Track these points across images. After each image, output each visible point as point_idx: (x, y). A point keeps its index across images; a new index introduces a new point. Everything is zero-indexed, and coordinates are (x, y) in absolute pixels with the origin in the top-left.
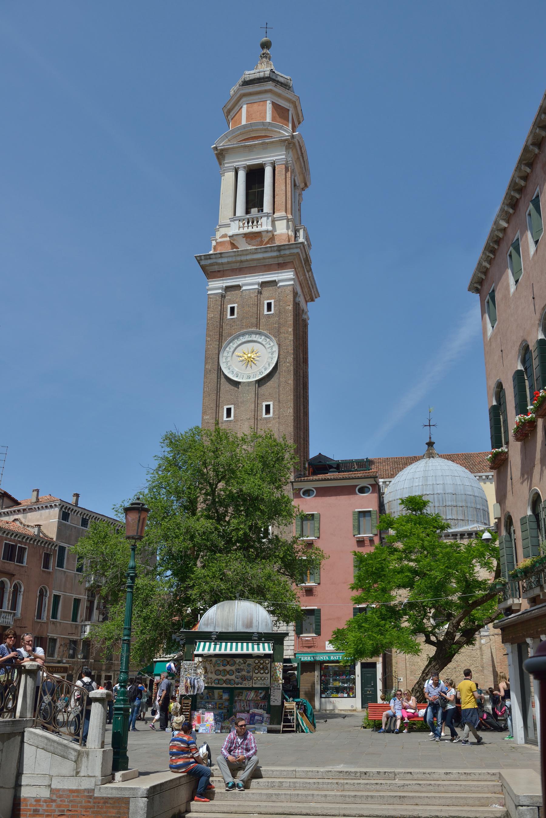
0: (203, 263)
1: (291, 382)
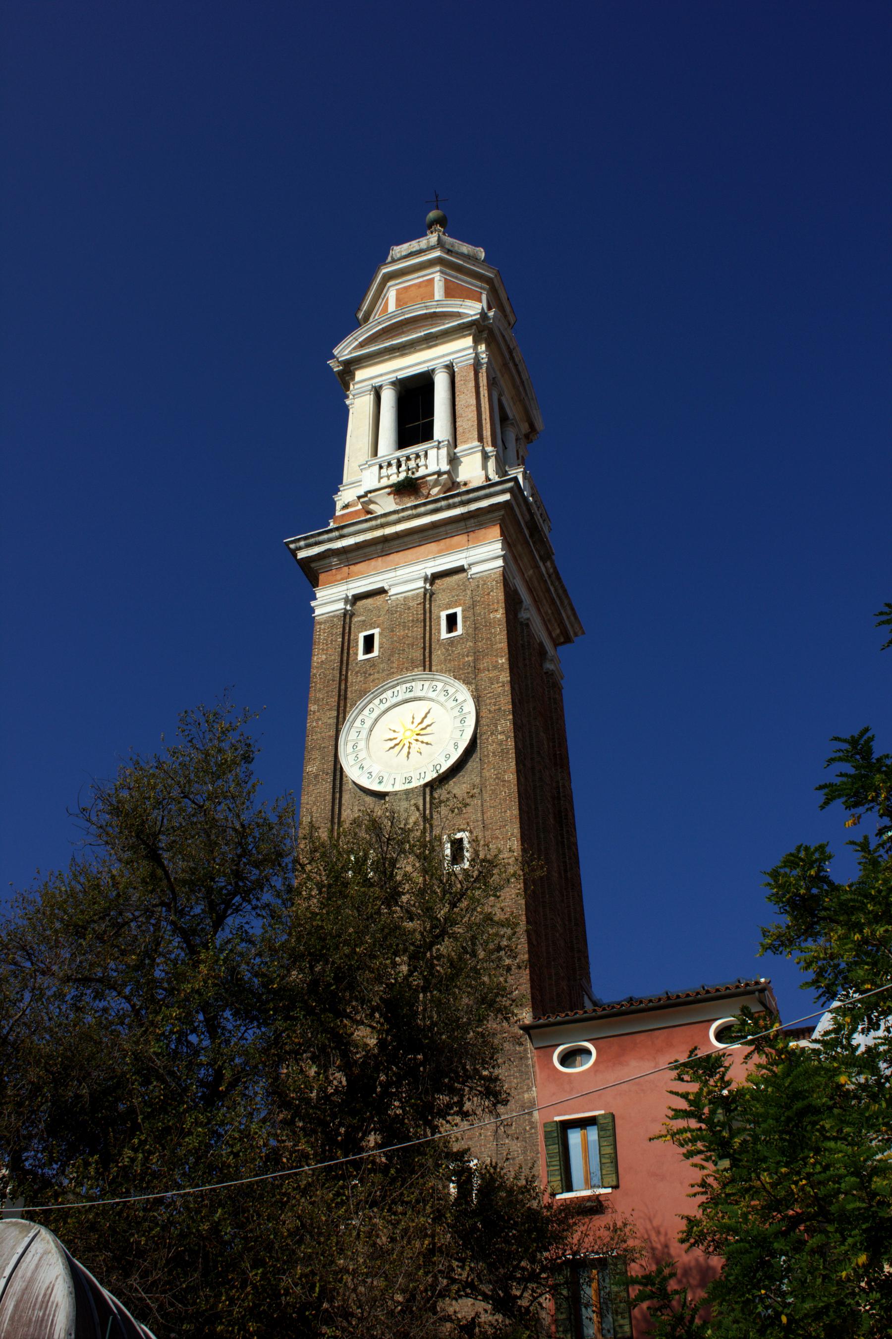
1: (511, 776)
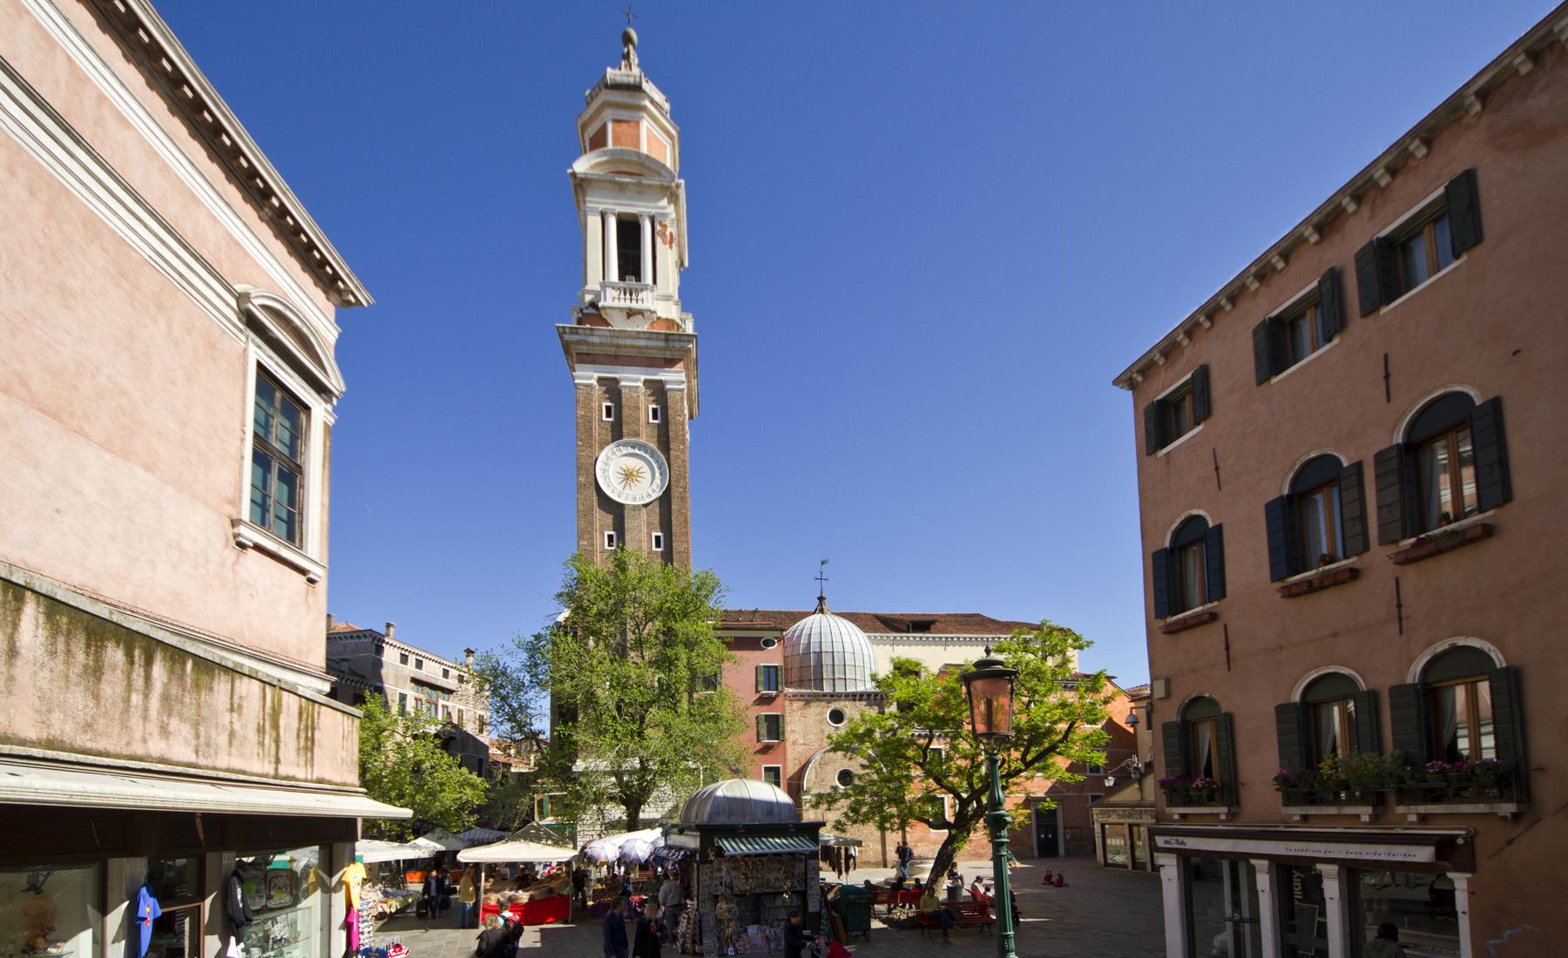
0: (567, 337)
